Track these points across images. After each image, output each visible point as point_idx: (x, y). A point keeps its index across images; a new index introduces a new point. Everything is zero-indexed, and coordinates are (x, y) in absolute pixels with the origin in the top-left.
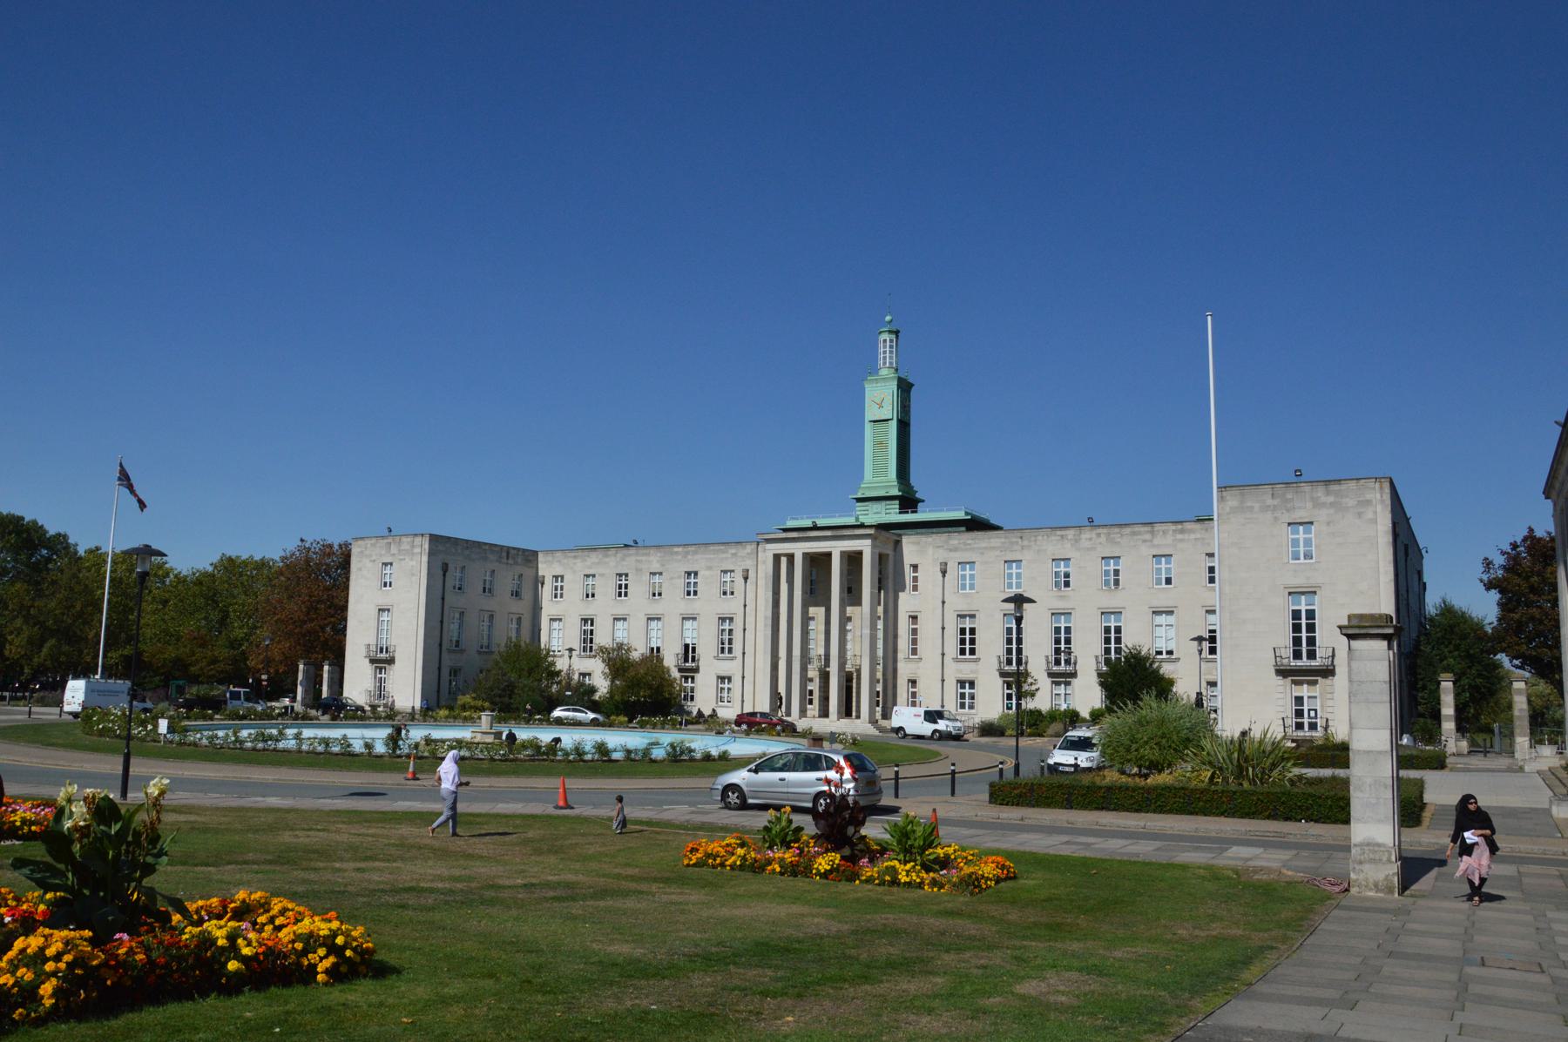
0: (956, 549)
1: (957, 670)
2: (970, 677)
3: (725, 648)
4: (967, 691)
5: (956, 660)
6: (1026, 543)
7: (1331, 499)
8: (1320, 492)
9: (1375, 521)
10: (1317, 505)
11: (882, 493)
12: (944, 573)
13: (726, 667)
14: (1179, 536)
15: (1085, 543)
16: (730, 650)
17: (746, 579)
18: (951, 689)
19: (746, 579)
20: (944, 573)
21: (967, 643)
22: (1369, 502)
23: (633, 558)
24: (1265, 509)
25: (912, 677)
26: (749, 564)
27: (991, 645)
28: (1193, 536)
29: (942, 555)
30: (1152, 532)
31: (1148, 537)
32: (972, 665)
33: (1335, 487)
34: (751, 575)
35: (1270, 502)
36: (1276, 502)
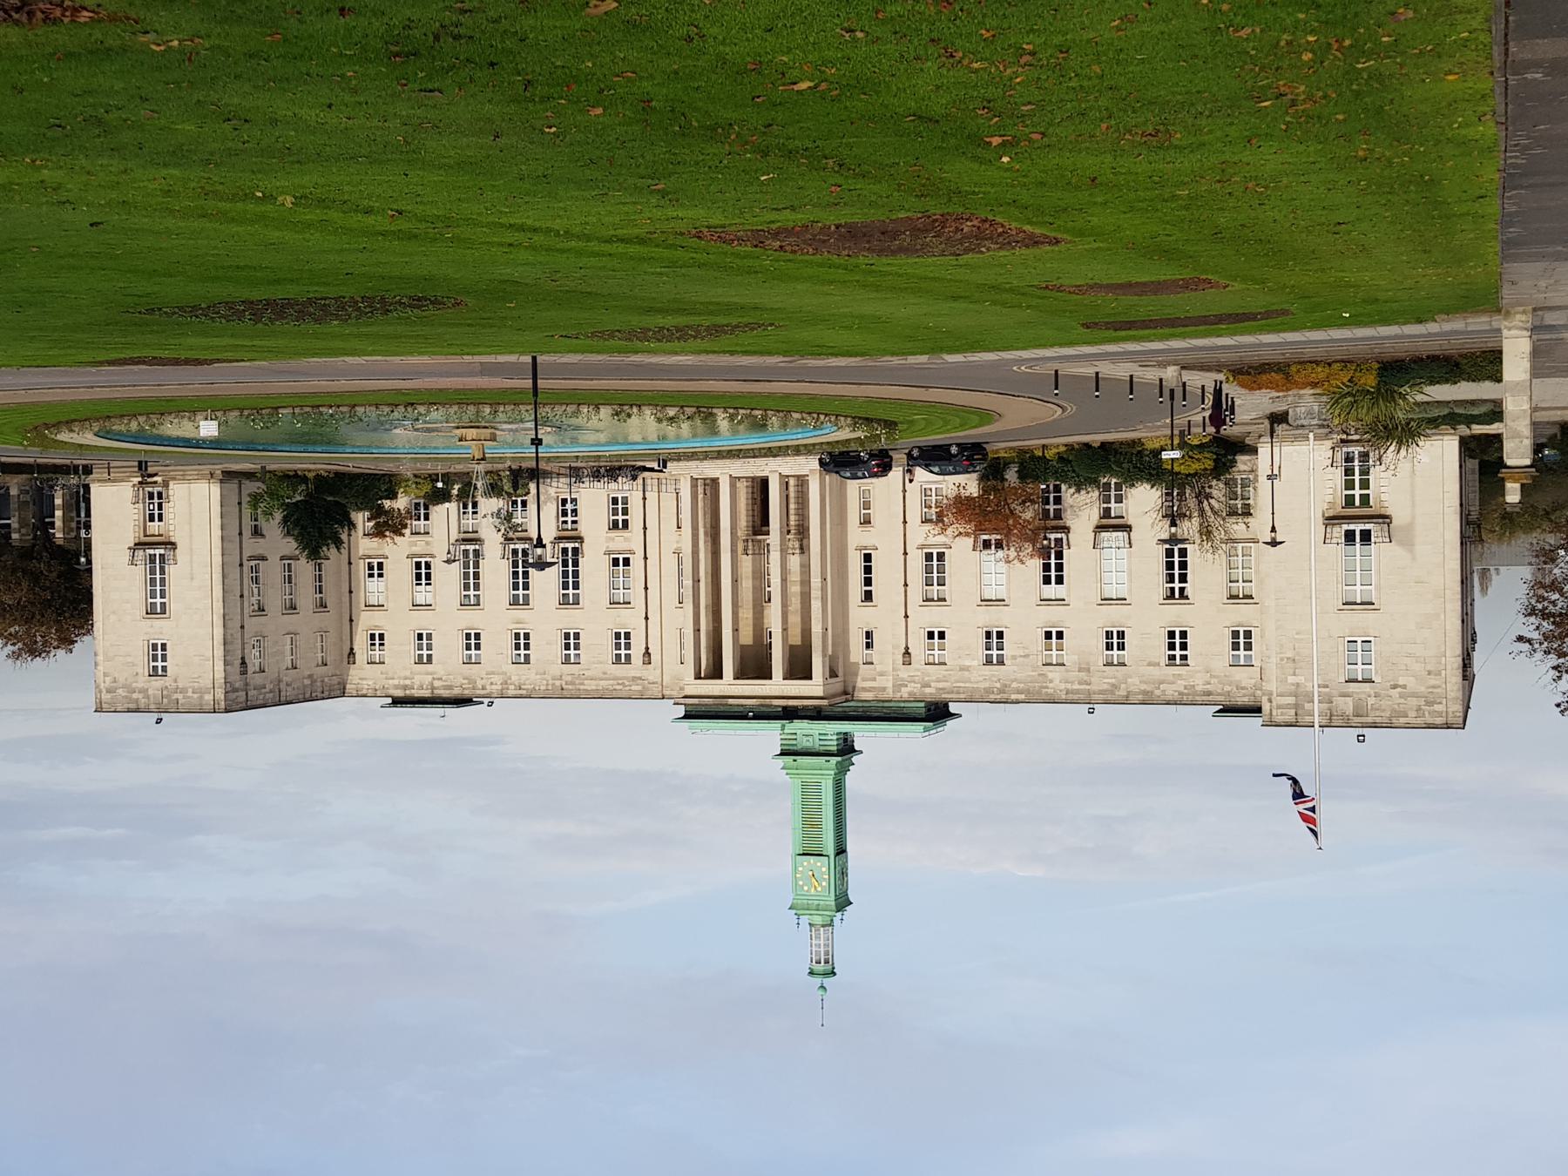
0: (634, 679)
1: (630, 541)
4: (620, 518)
6: (558, 683)
7: (135, 696)
8: (143, 703)
9: (105, 675)
10: (144, 691)
12: (647, 653)
14: (408, 682)
15: (497, 679)
16: (929, 557)
17: (907, 653)
18: (635, 518)
19: (907, 653)
20: (647, 653)
22: (108, 691)
23: (1094, 687)
24: (184, 691)
26: (905, 672)
27: (593, 566)
28: (396, 682)
29: (651, 673)
30: (433, 688)
31: (437, 684)
32: (612, 547)
33: (132, 706)
35: (180, 696)
36: (175, 696)
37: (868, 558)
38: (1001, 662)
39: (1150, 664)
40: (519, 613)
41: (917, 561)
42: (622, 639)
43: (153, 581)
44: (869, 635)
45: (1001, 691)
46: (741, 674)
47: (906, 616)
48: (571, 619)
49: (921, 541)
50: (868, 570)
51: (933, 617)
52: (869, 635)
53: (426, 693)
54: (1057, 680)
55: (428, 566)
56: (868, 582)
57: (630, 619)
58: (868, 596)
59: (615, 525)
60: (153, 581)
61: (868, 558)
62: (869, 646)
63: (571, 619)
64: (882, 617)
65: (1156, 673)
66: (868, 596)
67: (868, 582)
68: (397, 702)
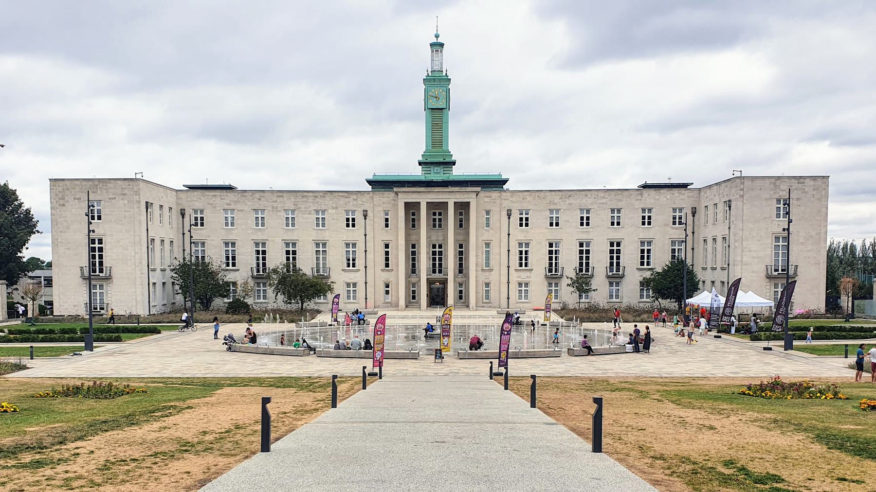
2: (527, 280)
3: (351, 263)
5: (516, 270)
11: (441, 160)
12: (509, 216)
13: (352, 277)
17: (365, 217)
19: (365, 217)
20: (509, 216)
21: (524, 259)
25: (487, 281)
32: (528, 274)
34: (370, 214)
37: (387, 265)
38: (317, 212)
39: (242, 211)
40: (584, 237)
41: (360, 263)
42: (524, 222)
43: (440, 259)
44: (387, 226)
45: (316, 197)
46: (445, 205)
47: (365, 235)
48: (553, 234)
49: (359, 273)
50: (387, 259)
51: (355, 235)
52: (387, 226)
53: (663, 191)
54: (289, 204)
55: (521, 265)
56: (387, 253)
57: (519, 234)
58: (387, 246)
59: (527, 285)
60: (440, 259)
61: (387, 265)
62: (387, 220)
63: (553, 234)
64: (378, 235)
65: (239, 207)
66: (387, 246)
67: (387, 253)
68: (684, 186)
